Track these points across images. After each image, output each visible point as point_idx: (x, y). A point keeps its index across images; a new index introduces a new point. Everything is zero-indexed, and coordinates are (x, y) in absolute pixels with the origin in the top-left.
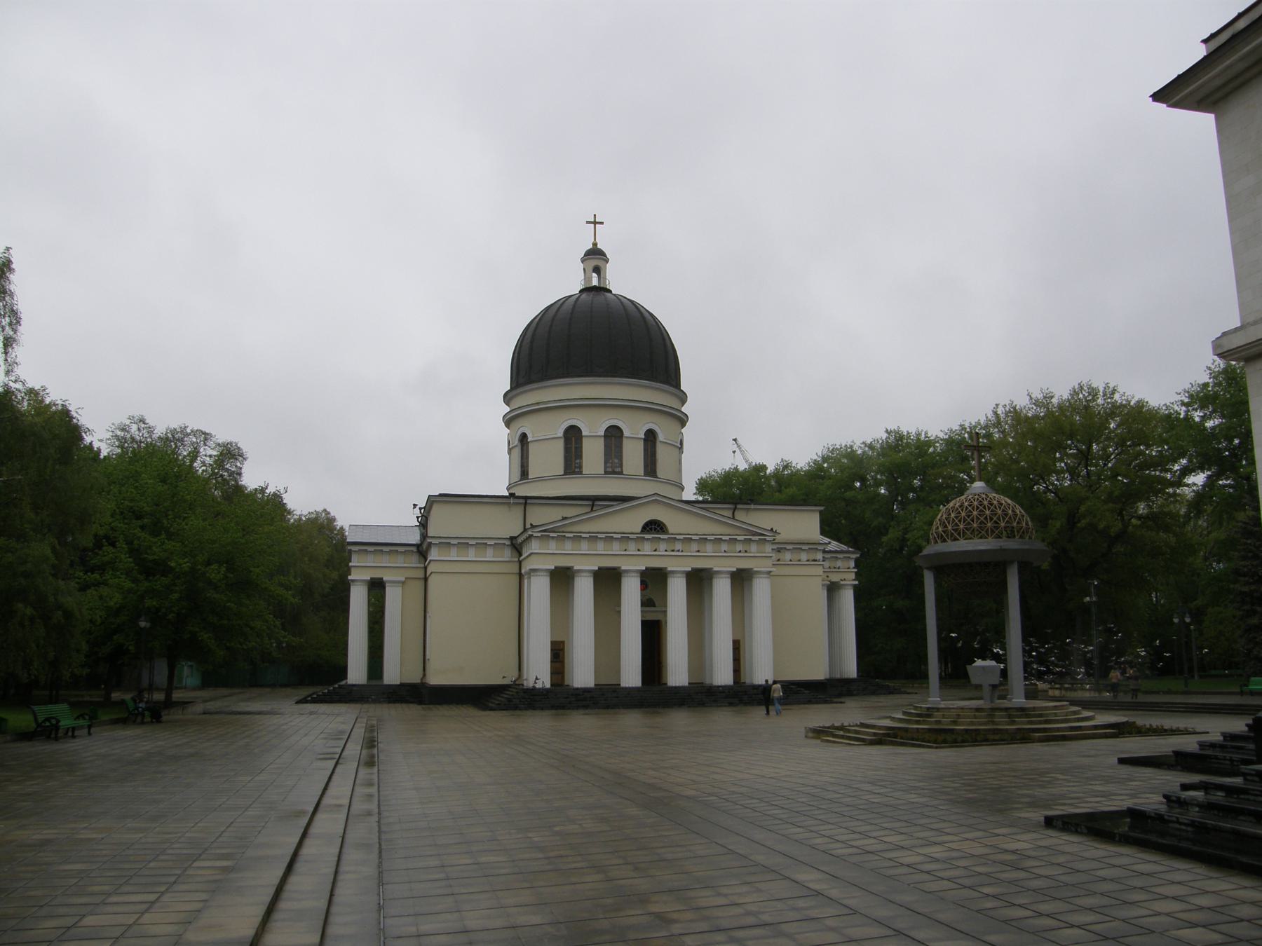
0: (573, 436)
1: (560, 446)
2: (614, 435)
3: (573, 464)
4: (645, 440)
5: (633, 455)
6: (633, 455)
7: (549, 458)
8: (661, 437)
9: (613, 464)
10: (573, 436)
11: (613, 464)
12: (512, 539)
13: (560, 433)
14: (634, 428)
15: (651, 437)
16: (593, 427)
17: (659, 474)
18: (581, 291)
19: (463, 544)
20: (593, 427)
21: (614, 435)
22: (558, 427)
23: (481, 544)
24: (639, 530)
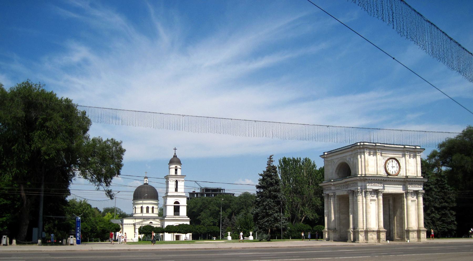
0: (142, 207)
1: (140, 209)
2: (148, 208)
3: (142, 211)
4: (152, 208)
5: (150, 210)
6: (150, 210)
7: (138, 211)
8: (155, 207)
9: (148, 211)
10: (142, 207)
11: (148, 211)
12: (134, 224)
13: (140, 207)
14: (150, 206)
15: (153, 208)
16: (145, 206)
17: (154, 212)
18: (144, 184)
19: (127, 224)
20: (145, 206)
21: (148, 208)
22: (140, 206)
23: (130, 224)
24: (149, 223)
